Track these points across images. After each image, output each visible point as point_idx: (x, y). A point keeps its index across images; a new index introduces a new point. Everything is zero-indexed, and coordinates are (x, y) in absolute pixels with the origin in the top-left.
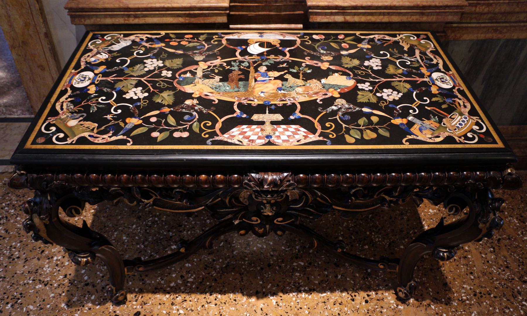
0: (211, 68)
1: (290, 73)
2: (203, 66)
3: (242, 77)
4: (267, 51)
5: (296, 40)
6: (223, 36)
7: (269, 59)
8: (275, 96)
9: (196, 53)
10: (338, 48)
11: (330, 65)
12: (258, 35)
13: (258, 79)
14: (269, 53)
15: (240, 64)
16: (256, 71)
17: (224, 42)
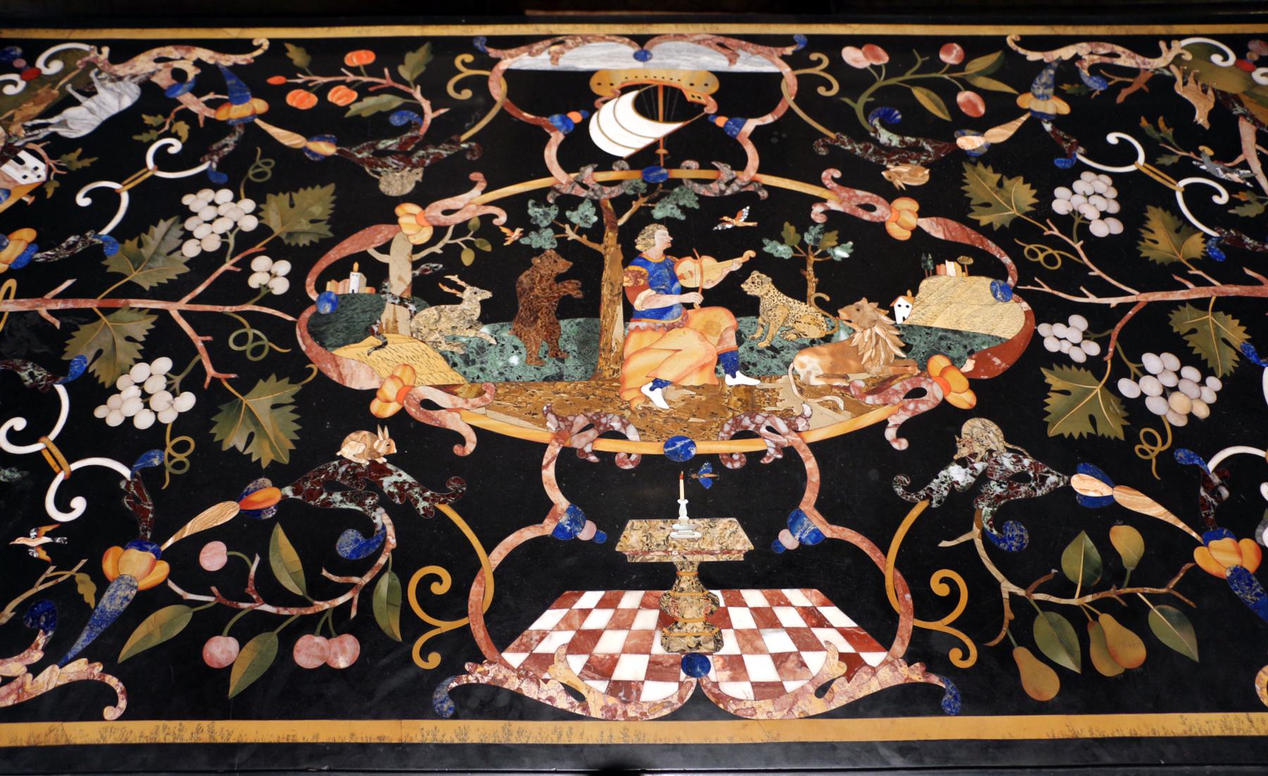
0: (446, 240)
1: (765, 263)
2: (413, 225)
3: (572, 289)
4: (670, 139)
5: (779, 76)
6: (493, 53)
7: (679, 182)
8: (709, 403)
9: (386, 153)
10: (947, 118)
11: (921, 214)
12: (629, 50)
13: (639, 304)
14: (677, 148)
15: (562, 218)
16: (630, 256)
17: (498, 89)
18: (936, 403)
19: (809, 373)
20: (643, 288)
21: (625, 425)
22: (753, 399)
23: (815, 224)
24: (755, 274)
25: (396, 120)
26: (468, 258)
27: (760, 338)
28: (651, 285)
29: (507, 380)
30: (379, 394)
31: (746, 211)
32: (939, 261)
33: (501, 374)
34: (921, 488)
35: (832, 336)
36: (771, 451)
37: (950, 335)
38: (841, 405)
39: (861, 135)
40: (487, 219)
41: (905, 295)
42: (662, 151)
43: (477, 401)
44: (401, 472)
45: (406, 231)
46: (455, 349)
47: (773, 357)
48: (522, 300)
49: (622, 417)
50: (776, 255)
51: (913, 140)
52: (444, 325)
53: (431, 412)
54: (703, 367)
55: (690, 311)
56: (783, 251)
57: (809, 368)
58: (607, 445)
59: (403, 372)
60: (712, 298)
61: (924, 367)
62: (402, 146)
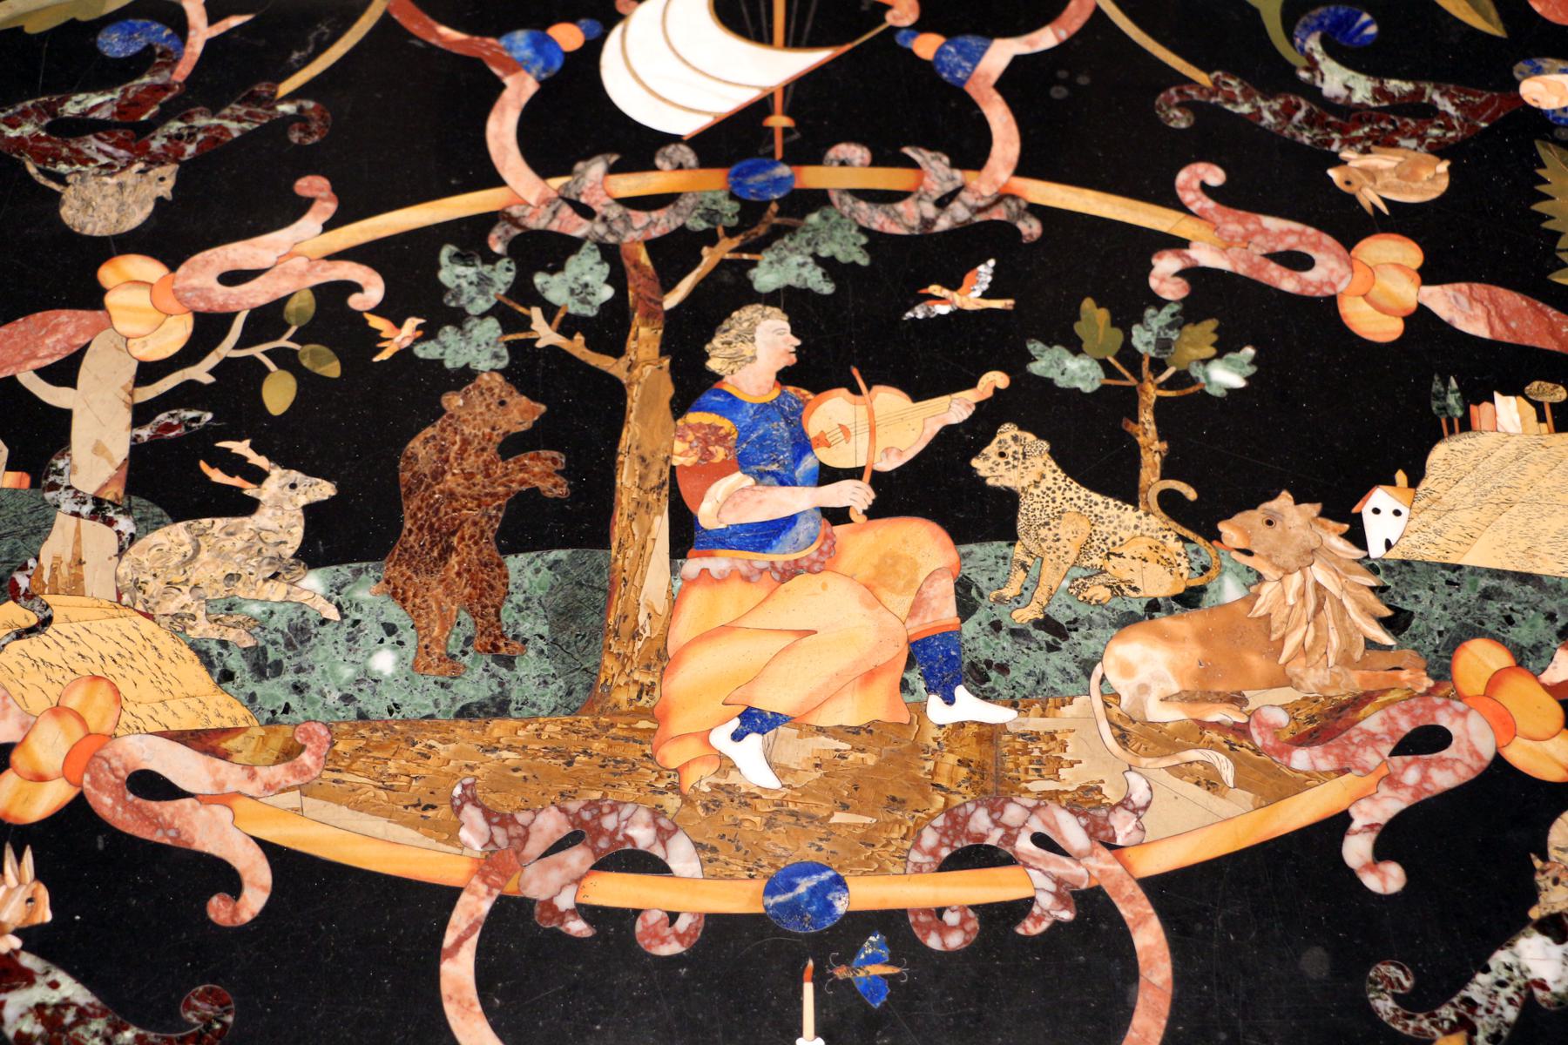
0: (227, 348)
1: (1034, 405)
2: (144, 312)
3: (543, 473)
4: (800, 91)
7: (819, 199)
8: (884, 772)
9: (84, 125)
10: (1495, 29)
11: (1429, 275)
13: (710, 512)
14: (817, 113)
15: (524, 292)
16: (693, 384)
18: (1479, 766)
19: (1144, 689)
20: (722, 471)
21: (664, 835)
22: (999, 760)
23: (1160, 303)
24: (1008, 431)
25: (113, 44)
26: (278, 394)
27: (1018, 599)
28: (743, 463)
29: (362, 716)
30: (17, 757)
31: (985, 272)
32: (1478, 393)
33: (347, 699)
34: (1445, 998)
35: (1202, 589)
36: (1045, 901)
37: (1509, 586)
38: (1227, 771)
39: (1275, 76)
40: (333, 295)
41: (1392, 483)
42: (779, 121)
43: (279, 773)
44: (60, 976)
45: (123, 325)
46: (231, 635)
47: (1052, 648)
48: (415, 503)
49: (657, 812)
50: (1061, 382)
51: (1408, 87)
52: (207, 571)
53: (155, 805)
54: (870, 676)
55: (839, 530)
56: (1077, 372)
57: (1142, 676)
58: (615, 890)
59: (89, 697)
60: (898, 494)
61: (1442, 672)
62: (127, 109)
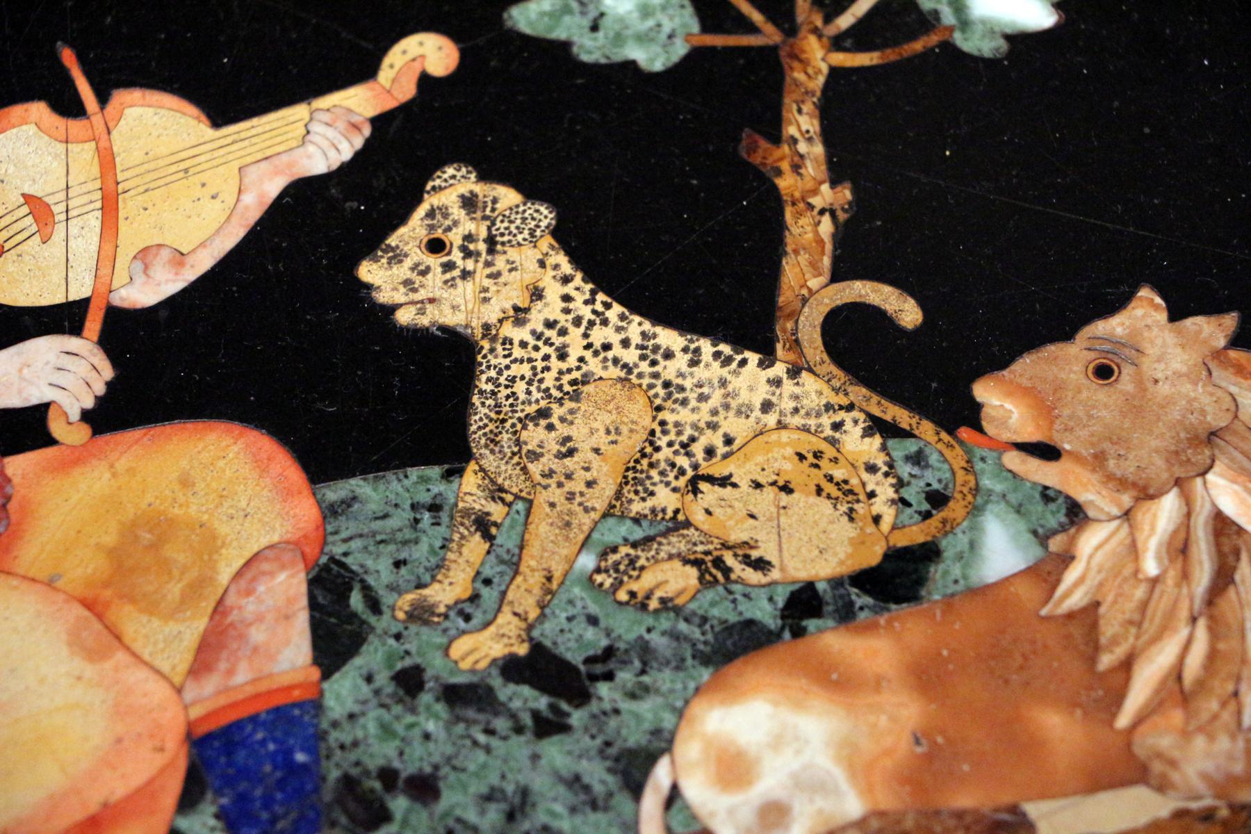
27: (465, 610)
35: (929, 553)
47: (548, 726)
57: (771, 781)
